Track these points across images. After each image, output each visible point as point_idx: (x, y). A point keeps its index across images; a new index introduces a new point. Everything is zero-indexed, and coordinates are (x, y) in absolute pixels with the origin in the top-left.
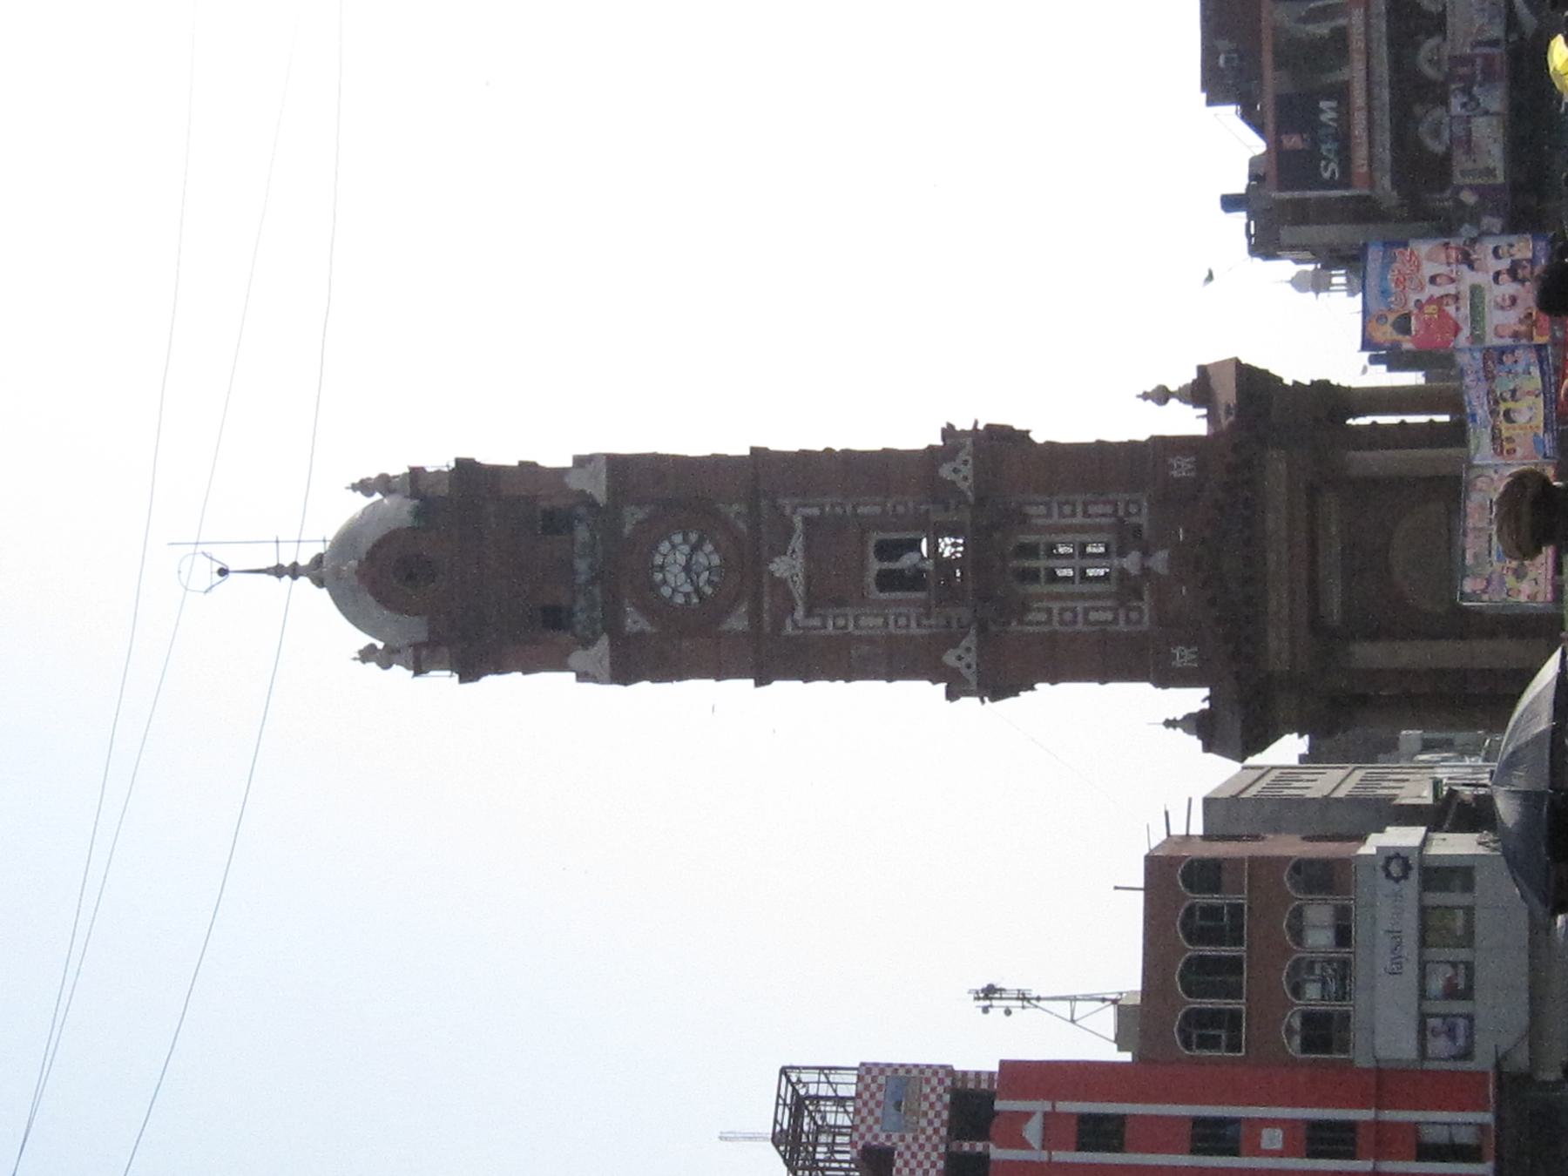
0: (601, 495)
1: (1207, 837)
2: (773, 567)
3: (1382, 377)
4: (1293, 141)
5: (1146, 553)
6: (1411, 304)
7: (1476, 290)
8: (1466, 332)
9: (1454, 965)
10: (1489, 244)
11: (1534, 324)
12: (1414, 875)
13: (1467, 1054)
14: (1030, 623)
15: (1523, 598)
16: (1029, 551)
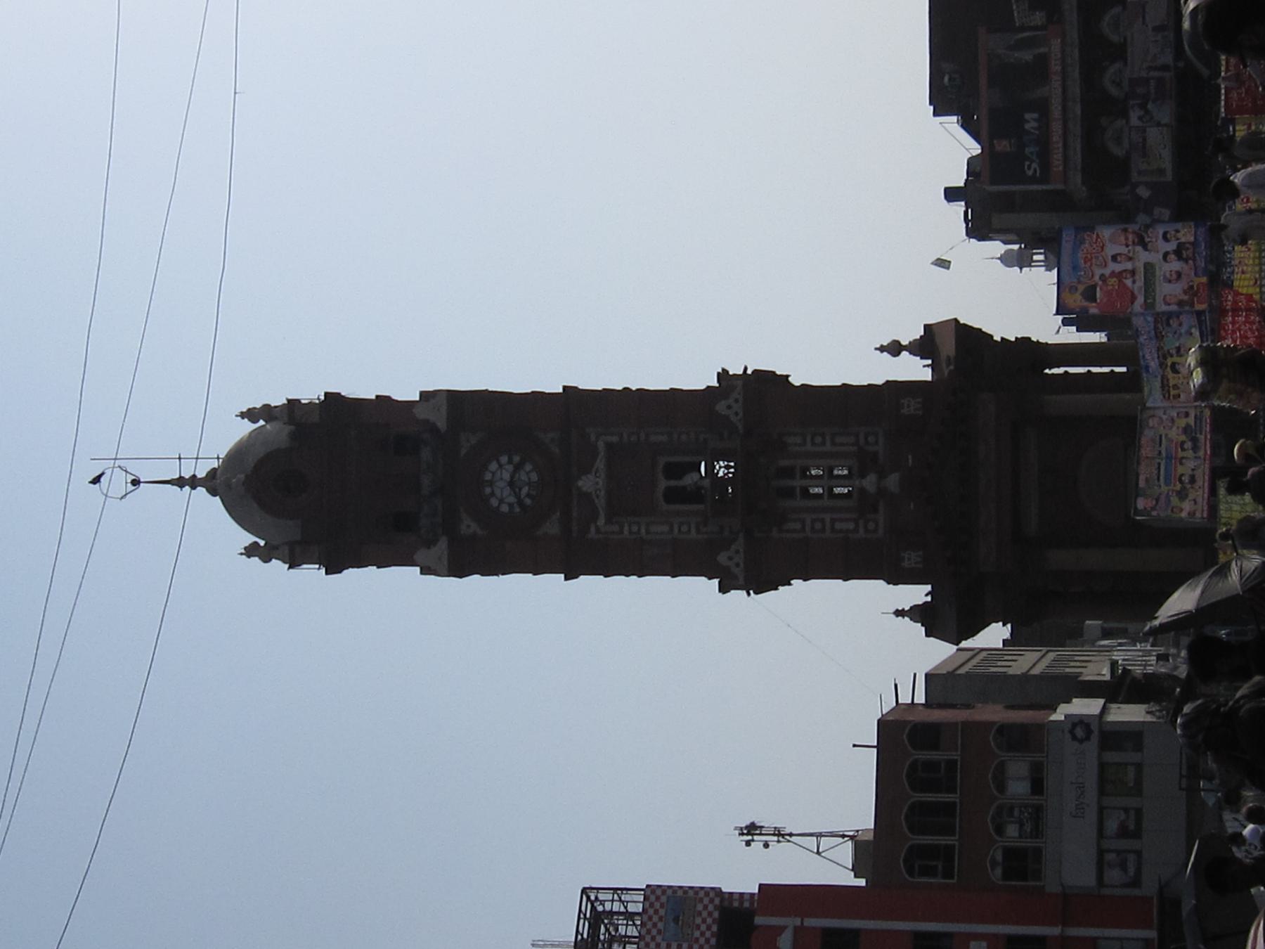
0: (442, 424)
1: (927, 705)
2: (580, 483)
3: (1071, 336)
4: (1003, 146)
6: (1097, 278)
7: (1149, 268)
8: (1140, 300)
9: (1126, 810)
10: (1160, 230)
11: (1196, 294)
12: (1095, 738)
13: (1136, 882)
14: (788, 531)
15: (1184, 515)
16: (788, 472)
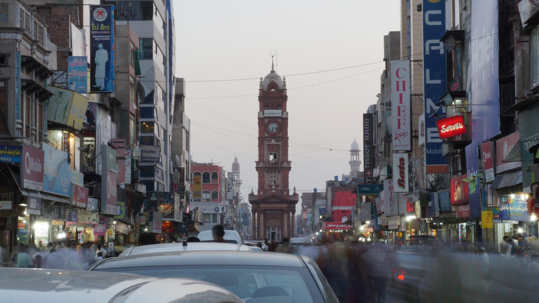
5: (274, 189)
